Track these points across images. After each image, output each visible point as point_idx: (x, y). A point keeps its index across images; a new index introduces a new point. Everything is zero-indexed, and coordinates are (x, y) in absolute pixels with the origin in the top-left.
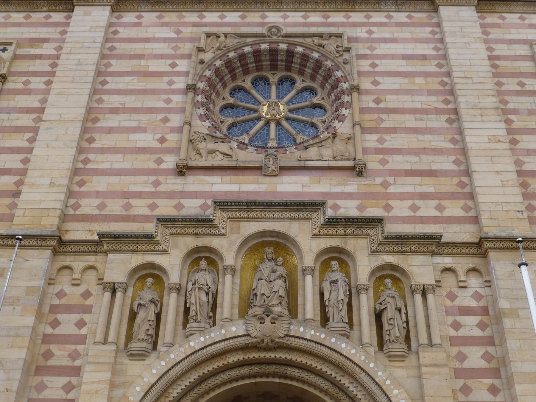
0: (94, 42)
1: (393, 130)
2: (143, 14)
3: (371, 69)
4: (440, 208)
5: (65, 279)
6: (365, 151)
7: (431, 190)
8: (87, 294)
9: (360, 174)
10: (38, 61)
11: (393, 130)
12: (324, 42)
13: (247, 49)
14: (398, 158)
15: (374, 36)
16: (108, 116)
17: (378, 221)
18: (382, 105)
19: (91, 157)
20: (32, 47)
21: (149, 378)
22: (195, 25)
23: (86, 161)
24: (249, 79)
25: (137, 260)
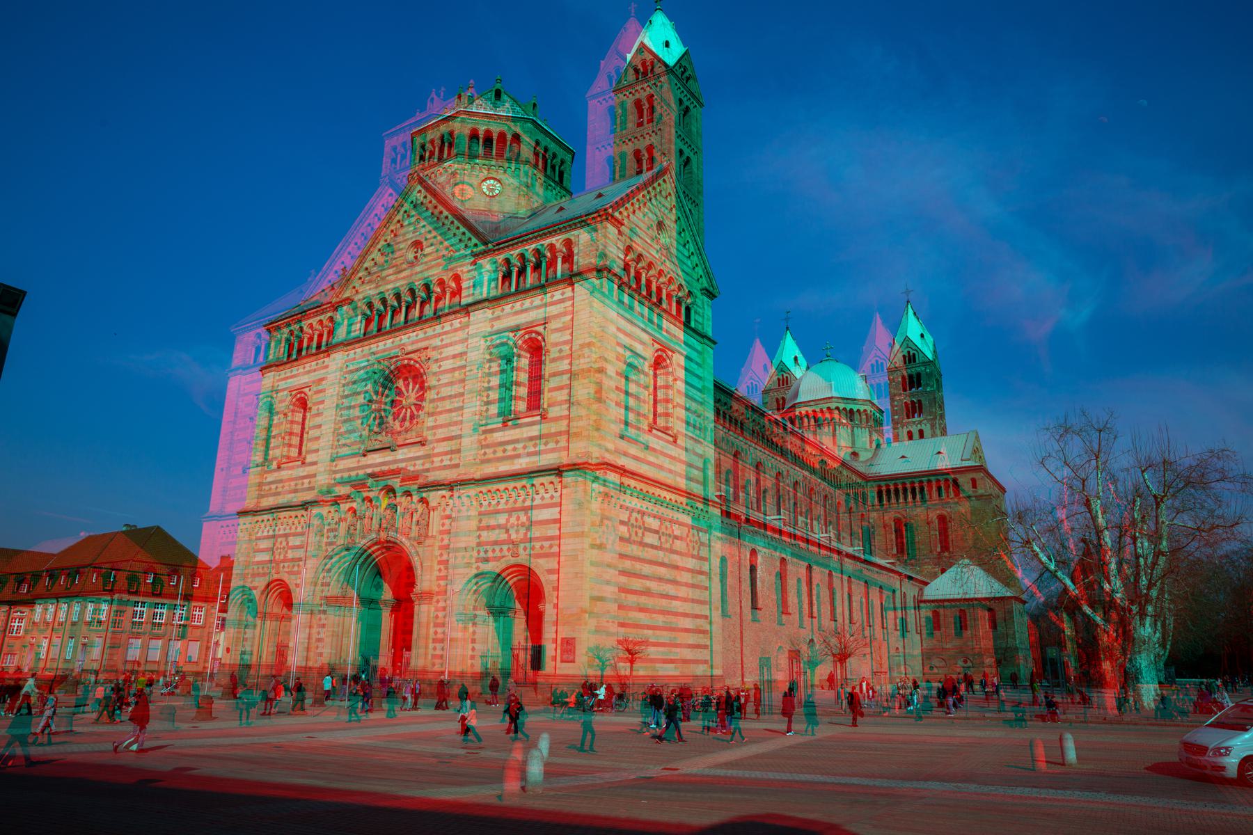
3: (438, 370)
4: (451, 459)
7: (449, 449)
8: (336, 523)
9: (423, 445)
11: (441, 413)
12: (421, 355)
13: (392, 367)
14: (440, 430)
15: (444, 343)
16: (344, 424)
17: (416, 478)
18: (439, 396)
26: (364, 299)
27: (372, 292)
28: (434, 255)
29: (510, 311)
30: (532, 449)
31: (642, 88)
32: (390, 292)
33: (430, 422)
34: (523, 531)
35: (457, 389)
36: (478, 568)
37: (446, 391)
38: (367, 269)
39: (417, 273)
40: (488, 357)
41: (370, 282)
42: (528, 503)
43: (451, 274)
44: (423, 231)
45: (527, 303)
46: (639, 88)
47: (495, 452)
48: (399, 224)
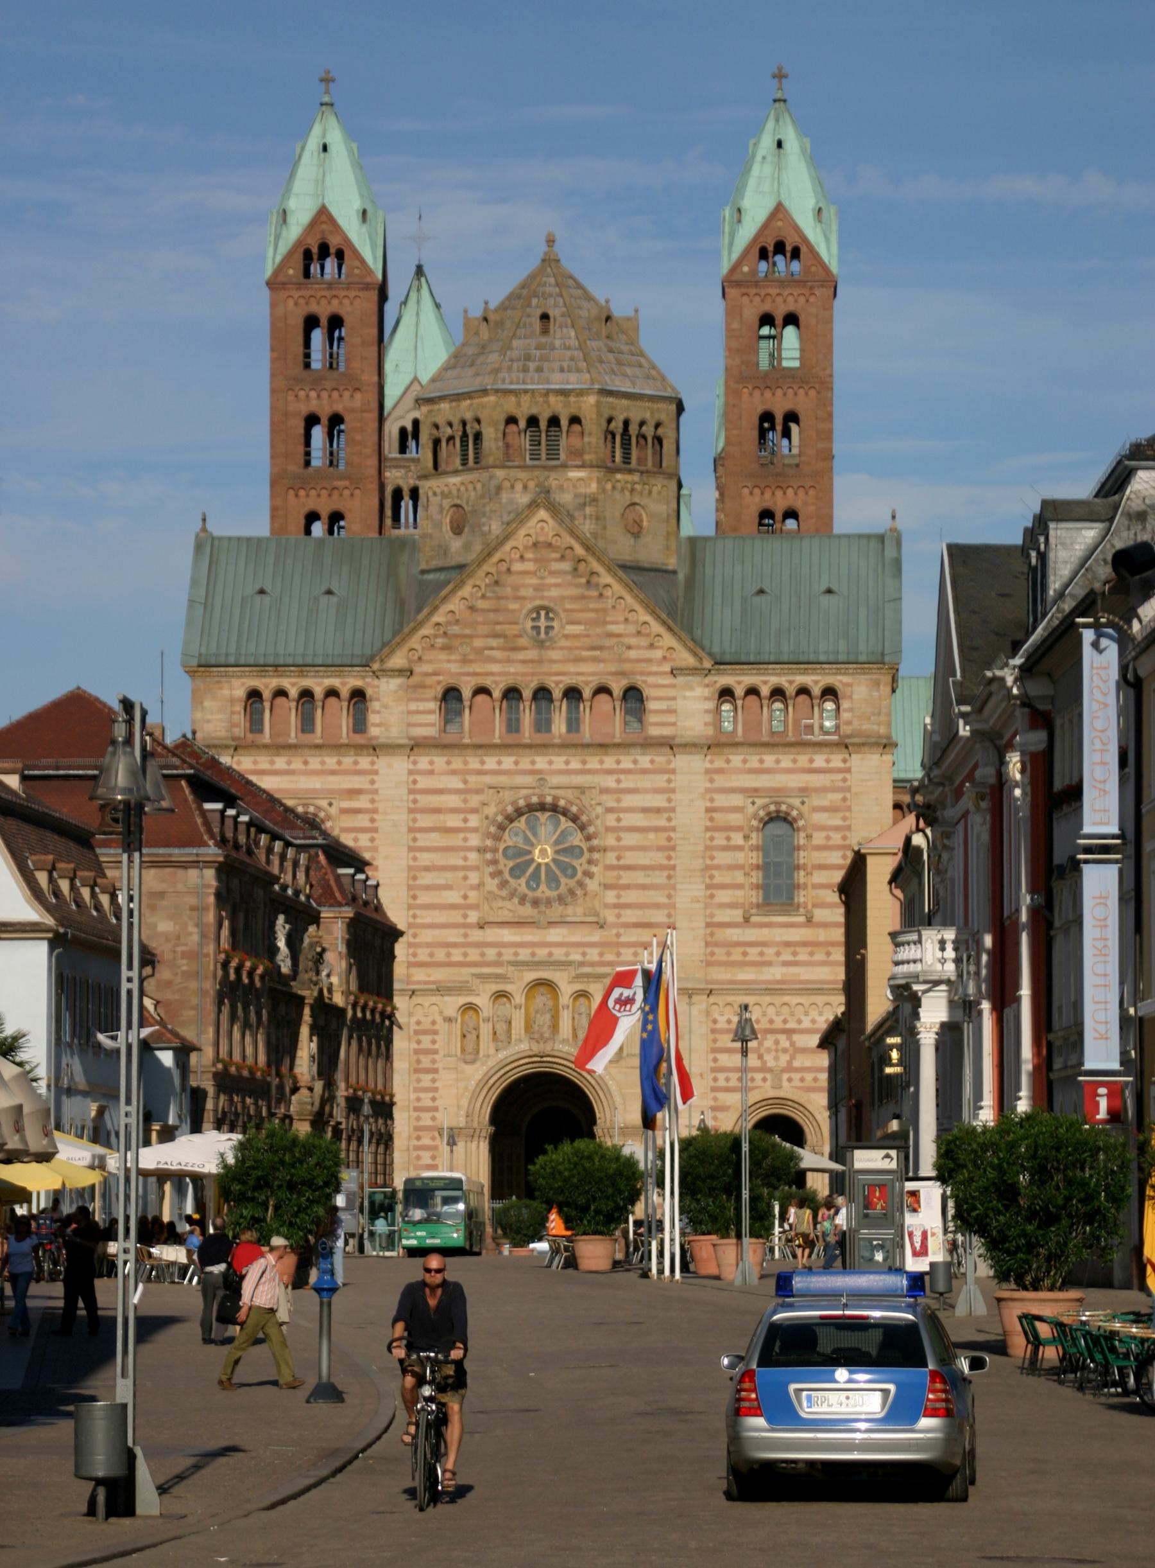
0: (402, 800)
1: (627, 887)
2: (436, 759)
5: (419, 1009)
6: (607, 906)
8: (434, 1023)
9: (602, 927)
10: (360, 816)
11: (627, 887)
12: (583, 797)
13: (522, 803)
15: (623, 785)
16: (424, 874)
18: (622, 862)
19: (418, 912)
20: (351, 799)
21: (478, 1076)
22: (479, 772)
23: (415, 916)
24: (523, 819)
25: (462, 1000)
26: (435, 673)
27: (454, 668)
28: (587, 642)
29: (740, 765)
30: (791, 958)
31: (778, 295)
32: (498, 678)
33: (611, 896)
34: (784, 1059)
35: (659, 858)
36: (715, 1099)
37: (630, 858)
38: (438, 624)
39: (552, 661)
40: (709, 824)
41: (446, 648)
42: (791, 1025)
43: (624, 683)
44: (554, 593)
45: (769, 760)
46: (773, 291)
47: (728, 954)
48: (503, 567)
